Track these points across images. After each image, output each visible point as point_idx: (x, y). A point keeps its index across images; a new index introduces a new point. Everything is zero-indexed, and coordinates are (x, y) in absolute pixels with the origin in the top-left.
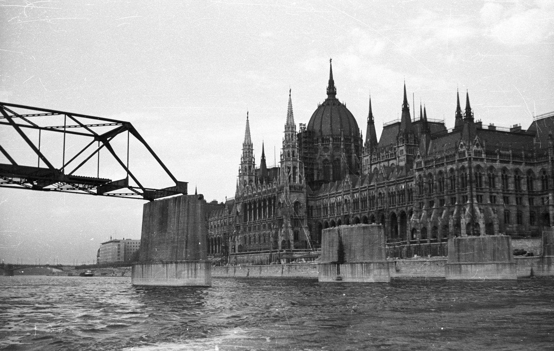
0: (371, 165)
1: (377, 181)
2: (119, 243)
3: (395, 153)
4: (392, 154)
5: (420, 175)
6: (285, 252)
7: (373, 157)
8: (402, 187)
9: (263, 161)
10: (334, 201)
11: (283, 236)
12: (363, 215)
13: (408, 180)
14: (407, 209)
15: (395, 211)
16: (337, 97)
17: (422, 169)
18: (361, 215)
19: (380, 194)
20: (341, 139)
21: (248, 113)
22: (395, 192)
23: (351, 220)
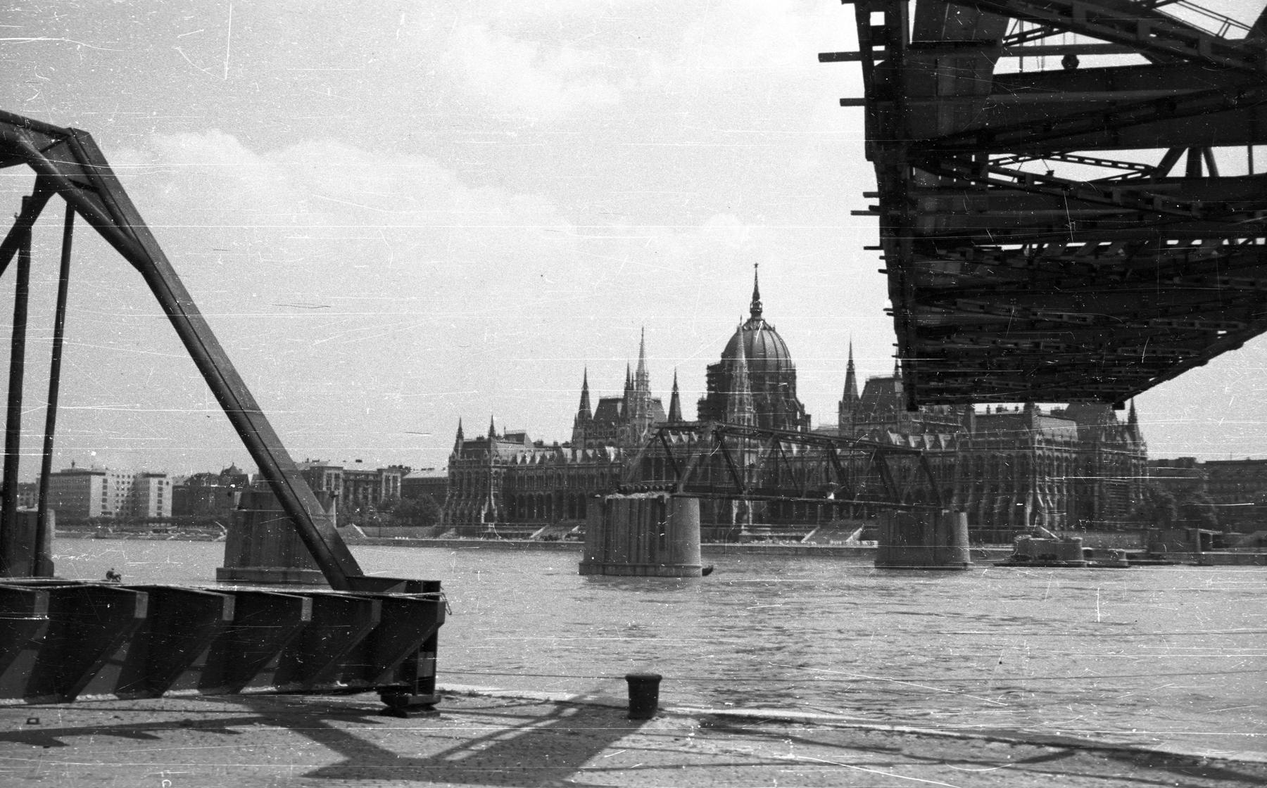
0: (854, 425)
3: (895, 417)
4: (889, 418)
5: (964, 457)
7: (858, 416)
16: (763, 316)
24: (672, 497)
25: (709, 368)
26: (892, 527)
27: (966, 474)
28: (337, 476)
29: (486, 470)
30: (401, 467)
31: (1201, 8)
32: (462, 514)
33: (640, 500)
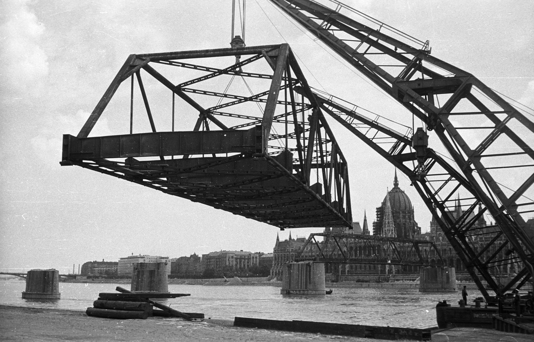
0: (437, 231)
2: (144, 259)
6: (391, 276)
16: (399, 186)
17: (483, 241)
18: (436, 258)
20: (406, 212)
24: (314, 263)
25: (377, 209)
26: (425, 274)
28: (232, 257)
29: (288, 253)
30: (260, 253)
31: (416, 42)
32: (279, 272)
33: (302, 264)
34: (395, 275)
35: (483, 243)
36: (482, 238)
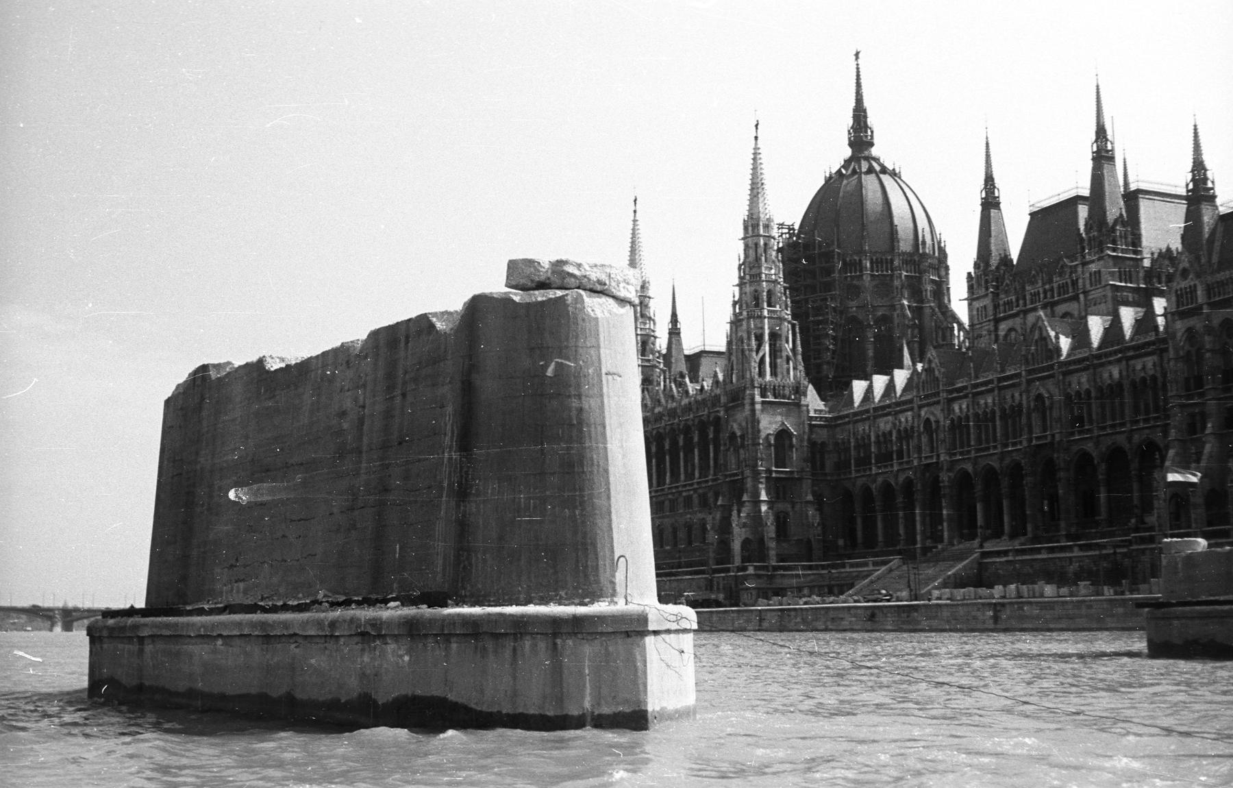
0: (997, 321)
1: (1027, 360)
3: (1075, 283)
4: (1063, 288)
5: (1189, 330)
6: (751, 571)
7: (1003, 298)
8: (1111, 376)
9: (674, 332)
10: (888, 427)
11: (744, 525)
12: (983, 463)
13: (1131, 353)
14: (1130, 439)
15: (1089, 447)
17: (1196, 311)
19: (1039, 397)
20: (892, 261)
21: (635, 200)
22: (1088, 392)
23: (946, 479)
27: (1199, 382)
34: (776, 568)
35: (1196, 323)
36: (1193, 290)
